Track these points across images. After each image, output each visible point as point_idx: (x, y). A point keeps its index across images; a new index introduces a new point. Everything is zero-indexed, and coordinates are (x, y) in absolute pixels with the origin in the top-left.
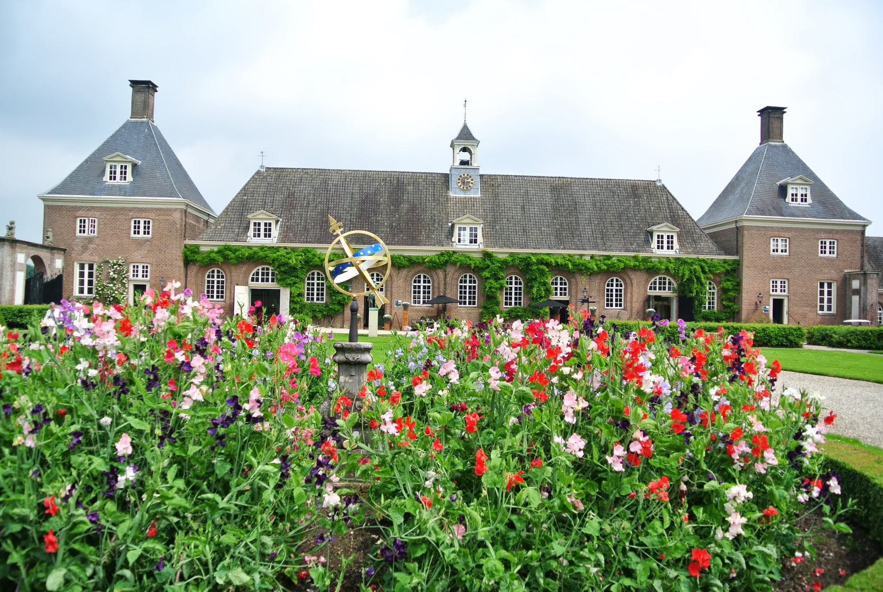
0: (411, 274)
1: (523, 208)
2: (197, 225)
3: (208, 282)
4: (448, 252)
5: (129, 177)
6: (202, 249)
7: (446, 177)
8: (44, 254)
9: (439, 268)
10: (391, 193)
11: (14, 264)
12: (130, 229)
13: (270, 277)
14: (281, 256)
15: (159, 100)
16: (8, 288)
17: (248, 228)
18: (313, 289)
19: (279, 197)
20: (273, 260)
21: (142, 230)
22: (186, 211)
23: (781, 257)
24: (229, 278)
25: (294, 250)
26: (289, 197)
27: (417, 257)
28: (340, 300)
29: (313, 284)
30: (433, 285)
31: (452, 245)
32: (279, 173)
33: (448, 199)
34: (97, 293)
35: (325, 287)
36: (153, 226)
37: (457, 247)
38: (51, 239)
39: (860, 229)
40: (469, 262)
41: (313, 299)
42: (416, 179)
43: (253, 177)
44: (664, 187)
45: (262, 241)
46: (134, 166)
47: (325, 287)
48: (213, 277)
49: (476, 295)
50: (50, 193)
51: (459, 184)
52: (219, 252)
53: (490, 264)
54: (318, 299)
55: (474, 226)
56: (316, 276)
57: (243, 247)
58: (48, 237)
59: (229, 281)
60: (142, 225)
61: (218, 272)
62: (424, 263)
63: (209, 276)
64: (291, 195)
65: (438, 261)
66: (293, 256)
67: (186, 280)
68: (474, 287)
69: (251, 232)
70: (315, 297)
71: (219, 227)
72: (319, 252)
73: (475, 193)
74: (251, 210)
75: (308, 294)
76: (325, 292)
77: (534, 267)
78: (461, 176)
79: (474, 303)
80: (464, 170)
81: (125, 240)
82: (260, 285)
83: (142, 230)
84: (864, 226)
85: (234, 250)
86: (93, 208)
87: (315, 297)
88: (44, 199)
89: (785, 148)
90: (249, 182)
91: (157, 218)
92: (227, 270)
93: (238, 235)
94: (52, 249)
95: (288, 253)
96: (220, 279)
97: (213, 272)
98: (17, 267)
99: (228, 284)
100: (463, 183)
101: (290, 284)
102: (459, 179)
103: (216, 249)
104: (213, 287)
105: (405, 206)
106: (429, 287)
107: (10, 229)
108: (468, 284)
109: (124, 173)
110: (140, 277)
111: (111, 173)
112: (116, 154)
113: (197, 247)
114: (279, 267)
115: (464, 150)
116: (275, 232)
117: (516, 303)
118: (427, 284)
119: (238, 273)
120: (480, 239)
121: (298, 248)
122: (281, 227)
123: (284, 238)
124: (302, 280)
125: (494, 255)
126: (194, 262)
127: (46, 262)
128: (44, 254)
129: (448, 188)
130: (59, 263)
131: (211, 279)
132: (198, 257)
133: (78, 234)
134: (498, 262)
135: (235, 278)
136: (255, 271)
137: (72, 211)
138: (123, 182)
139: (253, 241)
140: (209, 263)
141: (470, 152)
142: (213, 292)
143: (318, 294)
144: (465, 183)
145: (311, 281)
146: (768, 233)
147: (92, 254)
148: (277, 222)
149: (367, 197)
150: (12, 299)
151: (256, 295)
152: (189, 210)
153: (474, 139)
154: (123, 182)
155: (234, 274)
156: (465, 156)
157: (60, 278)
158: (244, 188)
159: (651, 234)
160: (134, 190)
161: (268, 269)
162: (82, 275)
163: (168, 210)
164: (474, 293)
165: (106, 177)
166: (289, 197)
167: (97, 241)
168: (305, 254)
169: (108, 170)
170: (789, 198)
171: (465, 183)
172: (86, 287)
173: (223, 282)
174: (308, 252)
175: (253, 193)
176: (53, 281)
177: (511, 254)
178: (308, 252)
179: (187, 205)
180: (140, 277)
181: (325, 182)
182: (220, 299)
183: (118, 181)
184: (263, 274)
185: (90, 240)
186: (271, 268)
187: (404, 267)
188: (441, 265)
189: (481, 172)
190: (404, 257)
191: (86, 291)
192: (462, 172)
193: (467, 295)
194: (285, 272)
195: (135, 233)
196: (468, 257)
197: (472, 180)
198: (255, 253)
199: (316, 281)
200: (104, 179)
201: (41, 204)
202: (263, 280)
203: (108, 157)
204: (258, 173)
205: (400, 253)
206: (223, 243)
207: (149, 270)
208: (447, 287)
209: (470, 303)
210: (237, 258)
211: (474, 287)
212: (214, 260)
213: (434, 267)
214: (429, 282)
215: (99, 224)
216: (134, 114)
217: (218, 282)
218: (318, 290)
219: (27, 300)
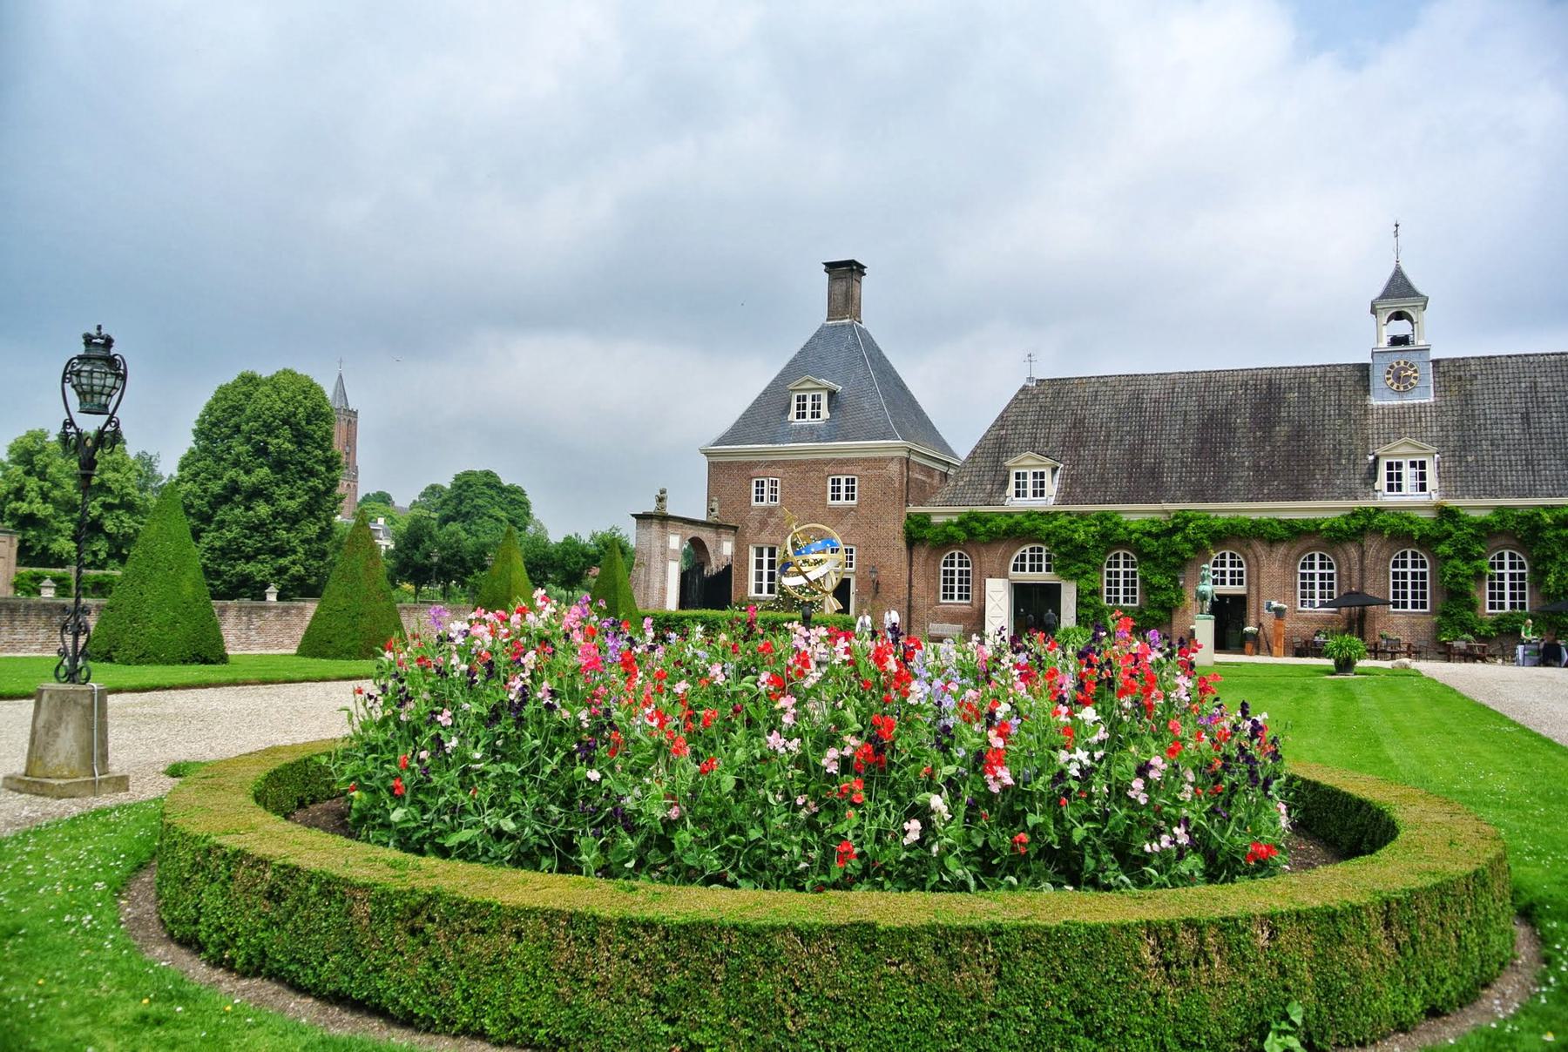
0: (1294, 553)
1: (1526, 418)
2: (929, 481)
3: (945, 572)
4: (1366, 510)
5: (825, 413)
6: (935, 520)
7: (1363, 370)
8: (706, 535)
9: (1352, 541)
10: (1256, 407)
11: (665, 547)
13: (1044, 563)
14: (1061, 527)
15: (868, 287)
16: (657, 585)
17: (1006, 483)
18: (1117, 583)
19: (1058, 428)
20: (1048, 535)
21: (843, 493)
22: (908, 460)
24: (977, 564)
25: (1082, 516)
26: (1075, 427)
27: (1305, 522)
28: (1163, 601)
29: (1117, 574)
30: (1339, 573)
31: (1374, 497)
32: (1058, 387)
33: (1366, 411)
34: (780, 592)
35: (1138, 579)
37: (1386, 499)
38: (716, 513)
40: (1408, 527)
41: (1117, 600)
42: (1303, 378)
43: (1016, 397)
45: (1030, 503)
46: (832, 394)
47: (1138, 579)
48: (952, 564)
49: (1428, 590)
50: (715, 445)
51: (1389, 382)
52: (960, 524)
53: (1452, 529)
54: (1126, 600)
56: (1121, 560)
57: (999, 514)
58: (713, 510)
59: (977, 571)
60: (843, 485)
61: (961, 556)
62: (1318, 531)
63: (945, 564)
64: (1078, 423)
65: (1345, 526)
66: (1081, 527)
67: (910, 571)
68: (1423, 575)
69: (1011, 489)
70: (1121, 596)
71: (961, 483)
72: (1125, 518)
73: (1422, 396)
74: (1012, 452)
75: (1109, 591)
76: (1138, 588)
77: (1550, 534)
78: (1392, 367)
79: (1423, 605)
80: (1398, 355)
82: (1028, 577)
83: (843, 493)
85: (983, 519)
86: (774, 463)
87: (1121, 596)
88: (708, 454)
90: (1009, 406)
91: (865, 473)
92: (974, 553)
93: (991, 495)
94: (716, 527)
95: (1071, 523)
96: (964, 568)
97: (952, 556)
98: (669, 553)
99: (977, 577)
100: (1398, 378)
101: (1076, 574)
102: (1389, 373)
103: (955, 519)
104: (952, 581)
105: (1282, 430)
106: (1331, 576)
107: (661, 500)
108: (1409, 570)
111: (798, 408)
112: (806, 377)
113: (927, 516)
114: (1057, 546)
115: (1399, 316)
116: (1052, 487)
117: (1513, 606)
118: (1327, 571)
119: (991, 558)
120: (1432, 481)
121: (1089, 513)
122: (1062, 475)
123: (1066, 496)
124: (1098, 568)
125: (1462, 512)
126: (923, 540)
127: (710, 547)
128: (706, 535)
129: (1367, 390)
130: (728, 548)
131: (949, 568)
132: (927, 533)
133: (754, 503)
134: (1470, 525)
135: (986, 566)
136: (1019, 553)
137: (745, 468)
138: (815, 422)
139: (1015, 503)
140: (944, 542)
141: (1411, 320)
142: (952, 589)
143: (1126, 592)
144: (1401, 379)
145: (1113, 569)
147: (772, 534)
148: (1054, 470)
149: (1211, 418)
150: (663, 601)
151: (1022, 594)
152: (914, 458)
153: (1415, 294)
154: (815, 422)
155: (985, 559)
156: (1401, 328)
157: (728, 568)
158: (1001, 417)
160: (834, 432)
161: (1040, 550)
162: (759, 564)
164: (1423, 585)
165: (792, 416)
166: (1075, 427)
168: (1101, 523)
169: (794, 403)
171: (1401, 379)
172: (765, 583)
173: (968, 573)
174: (1107, 519)
175: (1015, 423)
176: (718, 574)
177: (1499, 510)
178: (1107, 519)
179: (910, 450)
181: (1137, 397)
182: (964, 601)
183: (808, 420)
184: (1032, 558)
185: (770, 512)
186: (1045, 548)
187: (1281, 540)
188: (1354, 534)
189: (1434, 355)
190: (1280, 522)
191: (765, 588)
192: (1394, 359)
193: (1409, 590)
194: (1066, 555)
195: (833, 499)
196: (1407, 518)
197: (1415, 371)
198: (1018, 523)
199: (1122, 569)
201: (704, 461)
202: (1032, 569)
203: (797, 382)
204: (1024, 390)
205: (1272, 515)
206: (966, 509)
208: (1367, 574)
209: (1414, 605)
210: (989, 532)
211: (1423, 575)
212: (952, 537)
213: (1339, 538)
214: (1331, 567)
216: (832, 314)
217: (961, 573)
218: (1126, 583)
219: (683, 603)
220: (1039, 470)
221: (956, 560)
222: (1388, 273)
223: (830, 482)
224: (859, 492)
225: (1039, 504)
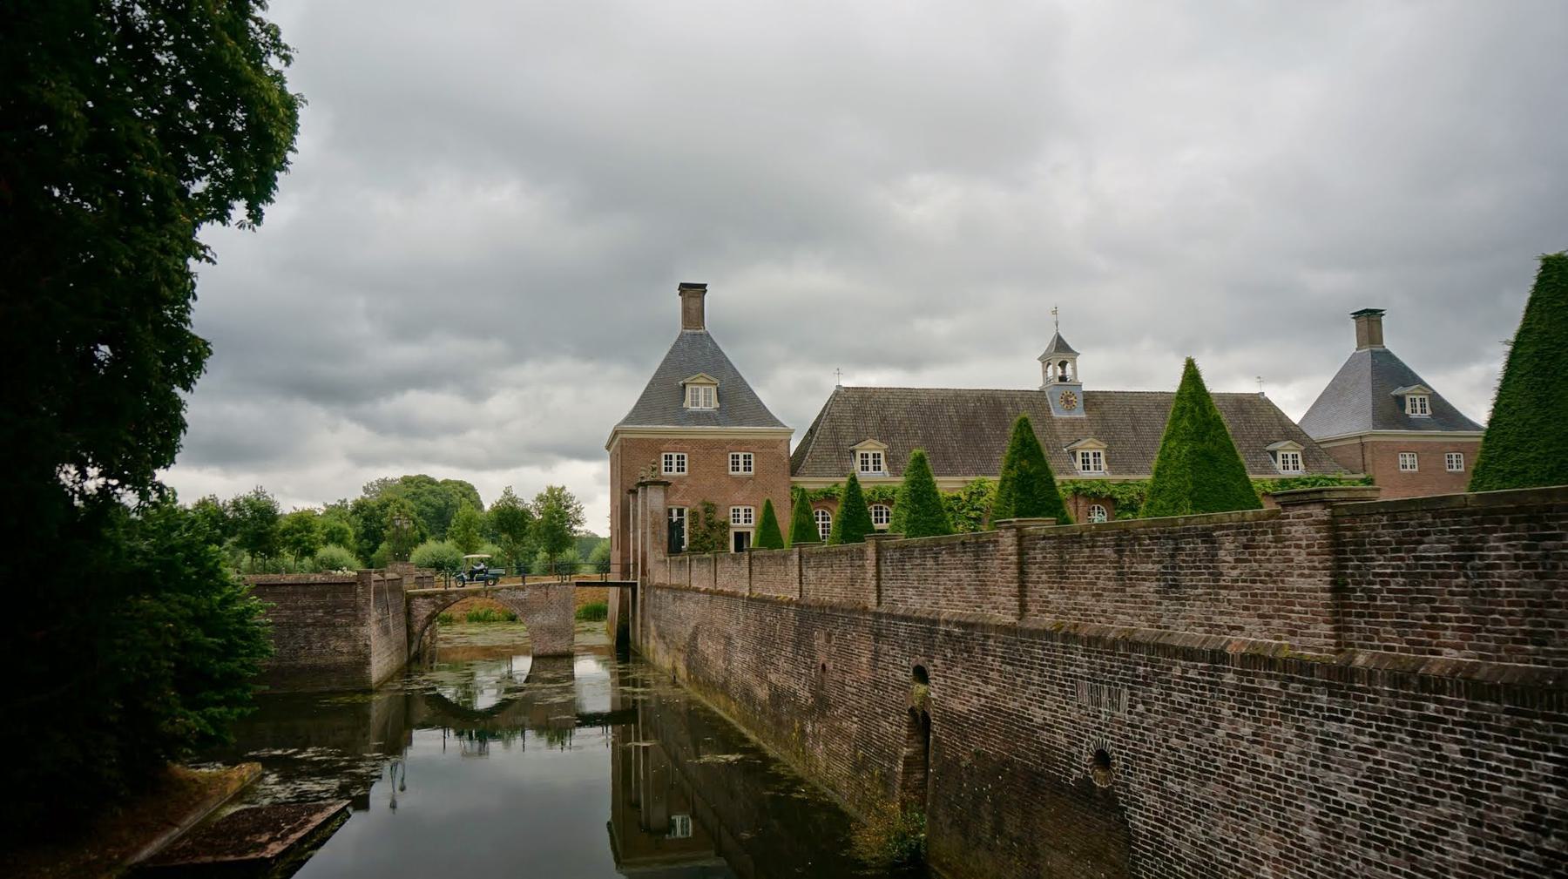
1: (1134, 428)
12: (728, 465)
13: (884, 517)
23: (1411, 473)
36: (756, 461)
44: (1268, 402)
60: (741, 460)
61: (823, 513)
64: (883, 419)
80: (1066, 388)
81: (724, 479)
89: (1387, 353)
100: (1067, 401)
110: (742, 523)
146: (1396, 450)
159: (1274, 454)
161: (881, 508)
163: (772, 441)
165: (687, 403)
167: (689, 481)
170: (1408, 411)
180: (742, 523)
183: (702, 407)
189: (1085, 388)
200: (684, 405)
207: (752, 513)
215: (689, 461)
217: (823, 525)
220: (876, 452)
221: (820, 516)
222: (1051, 336)
223: (730, 457)
224: (755, 465)
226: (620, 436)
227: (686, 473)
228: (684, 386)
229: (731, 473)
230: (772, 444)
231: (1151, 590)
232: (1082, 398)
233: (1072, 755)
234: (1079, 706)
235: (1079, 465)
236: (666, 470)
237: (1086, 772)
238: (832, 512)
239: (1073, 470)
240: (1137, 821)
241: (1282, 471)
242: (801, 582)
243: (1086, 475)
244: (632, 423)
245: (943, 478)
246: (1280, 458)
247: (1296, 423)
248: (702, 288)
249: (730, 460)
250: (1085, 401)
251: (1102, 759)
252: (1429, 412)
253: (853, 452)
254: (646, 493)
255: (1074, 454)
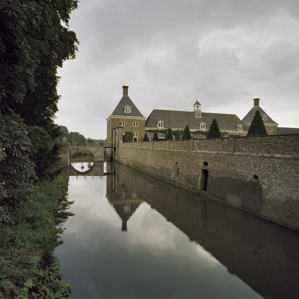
5: (130, 112)
36: (138, 124)
39: (277, 126)
44: (236, 116)
48: (150, 136)
55: (204, 125)
60: (136, 123)
61: (151, 135)
84: (278, 125)
89: (260, 107)
97: (150, 135)
109: (129, 110)
159: (237, 127)
161: (162, 134)
163: (142, 120)
165: (125, 111)
189: (202, 112)
202: (161, 137)
217: (151, 137)
221: (150, 135)
225: (162, 128)
226: (111, 117)
227: (124, 126)
228: (124, 108)
229: (133, 126)
230: (142, 120)
231: (269, 147)
232: (201, 114)
233: (248, 176)
234: (250, 168)
235: (200, 127)
236: (134, 125)
237: (252, 179)
238: (153, 135)
239: (199, 128)
240: (264, 187)
241: (238, 130)
242: (169, 147)
243: (201, 129)
244: (114, 115)
245: (173, 129)
246: (238, 128)
247: (241, 119)
248: (127, 87)
249: (133, 123)
250: (202, 114)
251: (256, 177)
252: (267, 120)
253: (157, 123)
254: (118, 129)
255: (200, 125)
